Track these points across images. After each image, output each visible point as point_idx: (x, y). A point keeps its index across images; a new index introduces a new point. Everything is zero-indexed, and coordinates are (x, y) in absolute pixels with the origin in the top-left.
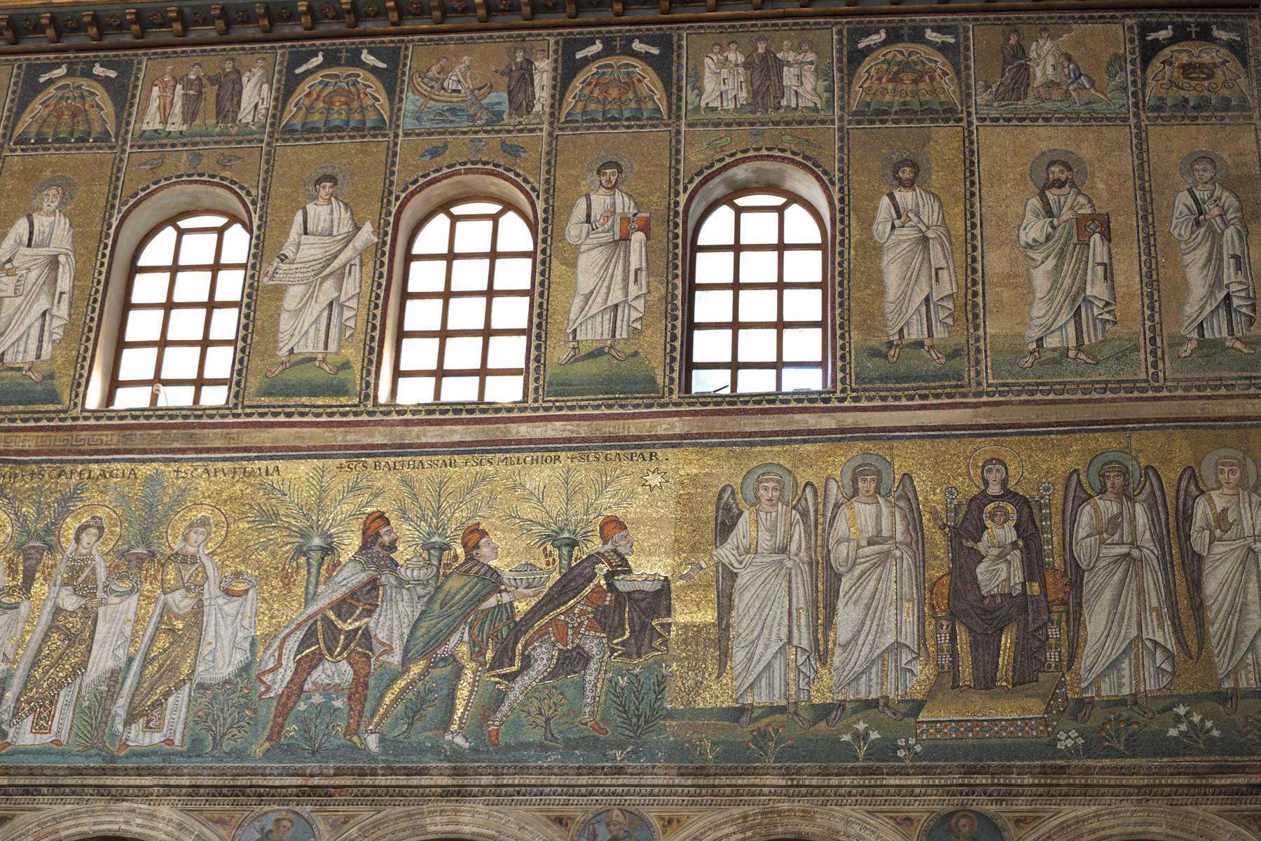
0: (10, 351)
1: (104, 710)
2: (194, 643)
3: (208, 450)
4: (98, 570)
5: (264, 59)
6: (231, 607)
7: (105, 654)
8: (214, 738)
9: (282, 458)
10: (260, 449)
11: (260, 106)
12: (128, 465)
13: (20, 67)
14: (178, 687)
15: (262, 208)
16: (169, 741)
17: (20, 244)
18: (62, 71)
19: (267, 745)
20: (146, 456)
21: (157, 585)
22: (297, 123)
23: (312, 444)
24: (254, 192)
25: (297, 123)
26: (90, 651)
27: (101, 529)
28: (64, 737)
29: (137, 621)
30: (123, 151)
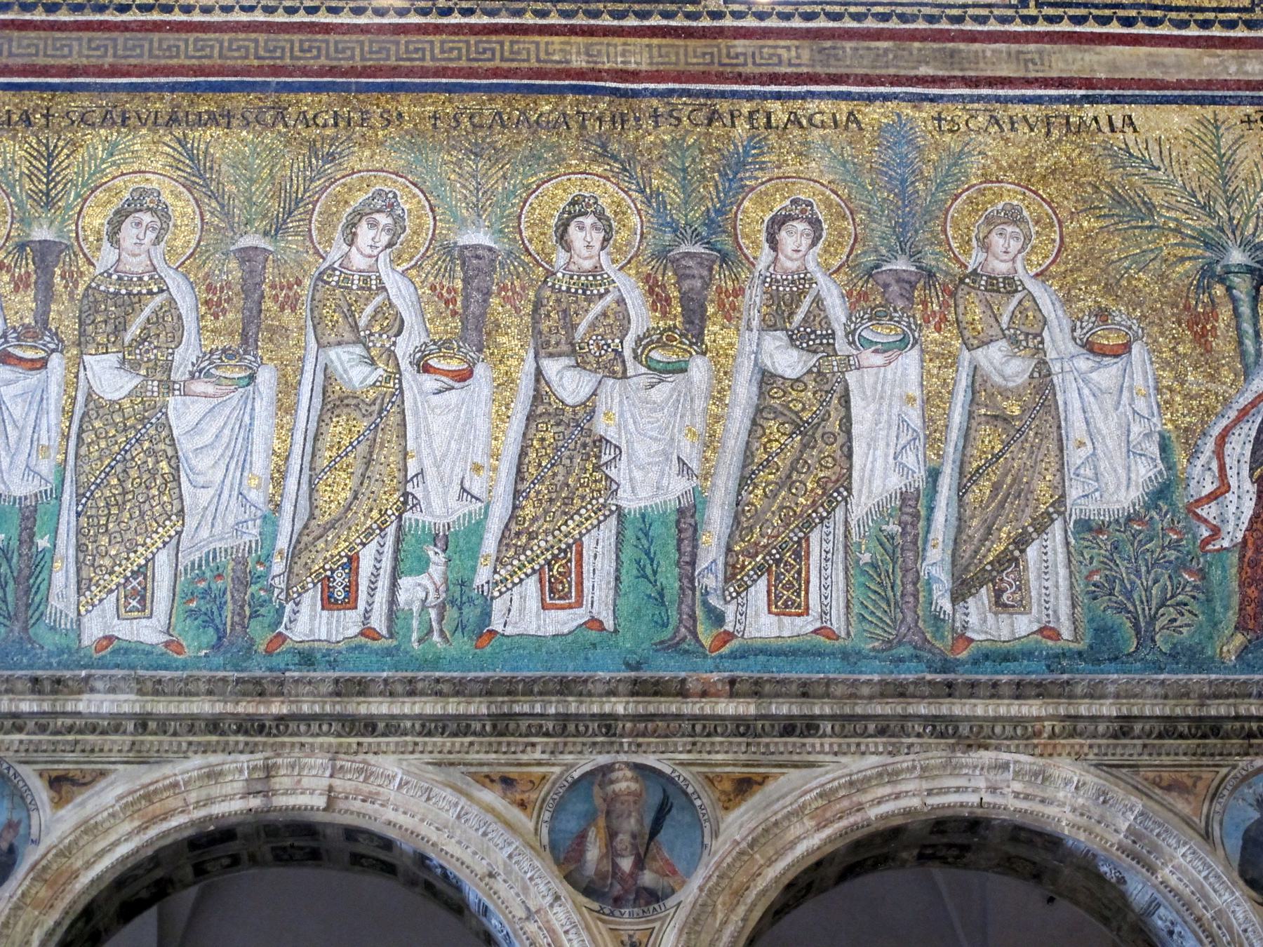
1: (906, 571)
2: (1053, 446)
3: (992, 82)
4: (828, 302)
6: (1107, 374)
7: (879, 464)
8: (1136, 626)
9: (1134, 100)
10: (1088, 83)
14: (1041, 525)
16: (1048, 631)
19: (1239, 639)
20: (872, 89)
21: (950, 332)
23: (1184, 76)
26: (849, 456)
27: (815, 223)
28: (837, 622)
29: (927, 401)
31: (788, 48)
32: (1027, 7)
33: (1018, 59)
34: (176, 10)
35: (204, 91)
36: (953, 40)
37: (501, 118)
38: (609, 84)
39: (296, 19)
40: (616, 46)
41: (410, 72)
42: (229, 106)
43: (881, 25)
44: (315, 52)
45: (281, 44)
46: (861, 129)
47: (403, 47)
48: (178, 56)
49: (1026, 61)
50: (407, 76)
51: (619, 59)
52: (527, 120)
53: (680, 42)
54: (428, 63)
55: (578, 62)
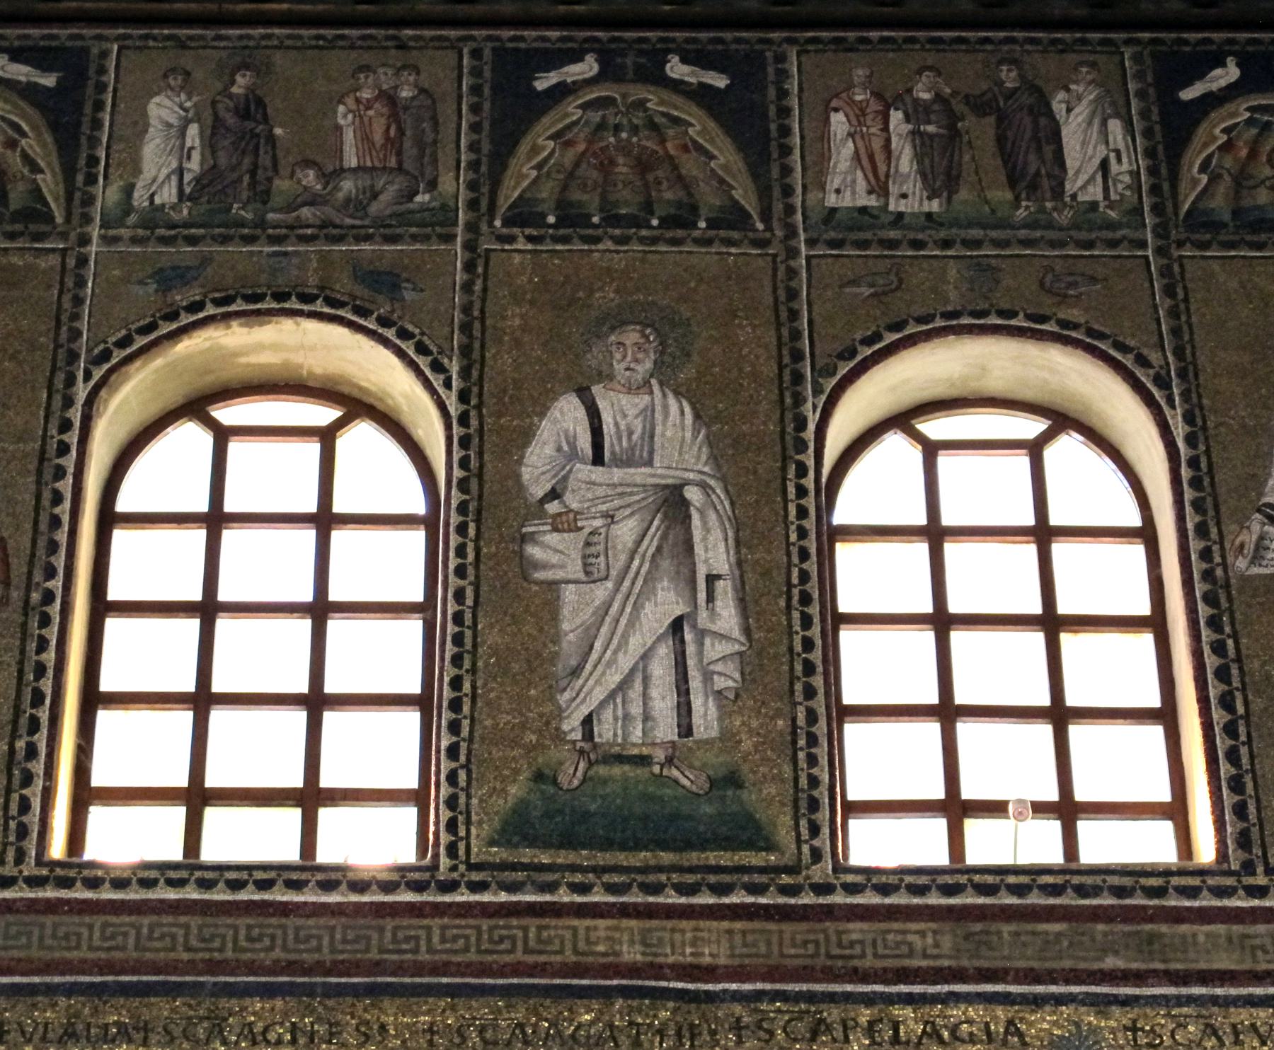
0: (607, 715)
3: (1205, 978)
5: (1093, 65)
11: (1114, 167)
12: (1000, 1012)
13: (476, 54)
15: (1186, 395)
17: (573, 455)
18: (587, 67)
20: (1040, 989)
22: (1219, 203)
24: (1154, 357)
25: (1219, 203)
30: (793, 253)
31: (922, 934)
32: (1254, 874)
33: (1243, 948)
34: (79, 884)
35: (113, 995)
36: (1151, 920)
37: (524, 1033)
38: (673, 985)
39: (243, 896)
40: (683, 931)
41: (399, 969)
42: (146, 1016)
43: (1052, 901)
44: (267, 942)
45: (222, 931)
46: (1025, 1044)
47: (388, 935)
48: (78, 947)
49: (1253, 948)
50: (393, 974)
51: (688, 950)
52: (559, 1033)
53: (772, 926)
54: (424, 957)
55: (631, 954)
